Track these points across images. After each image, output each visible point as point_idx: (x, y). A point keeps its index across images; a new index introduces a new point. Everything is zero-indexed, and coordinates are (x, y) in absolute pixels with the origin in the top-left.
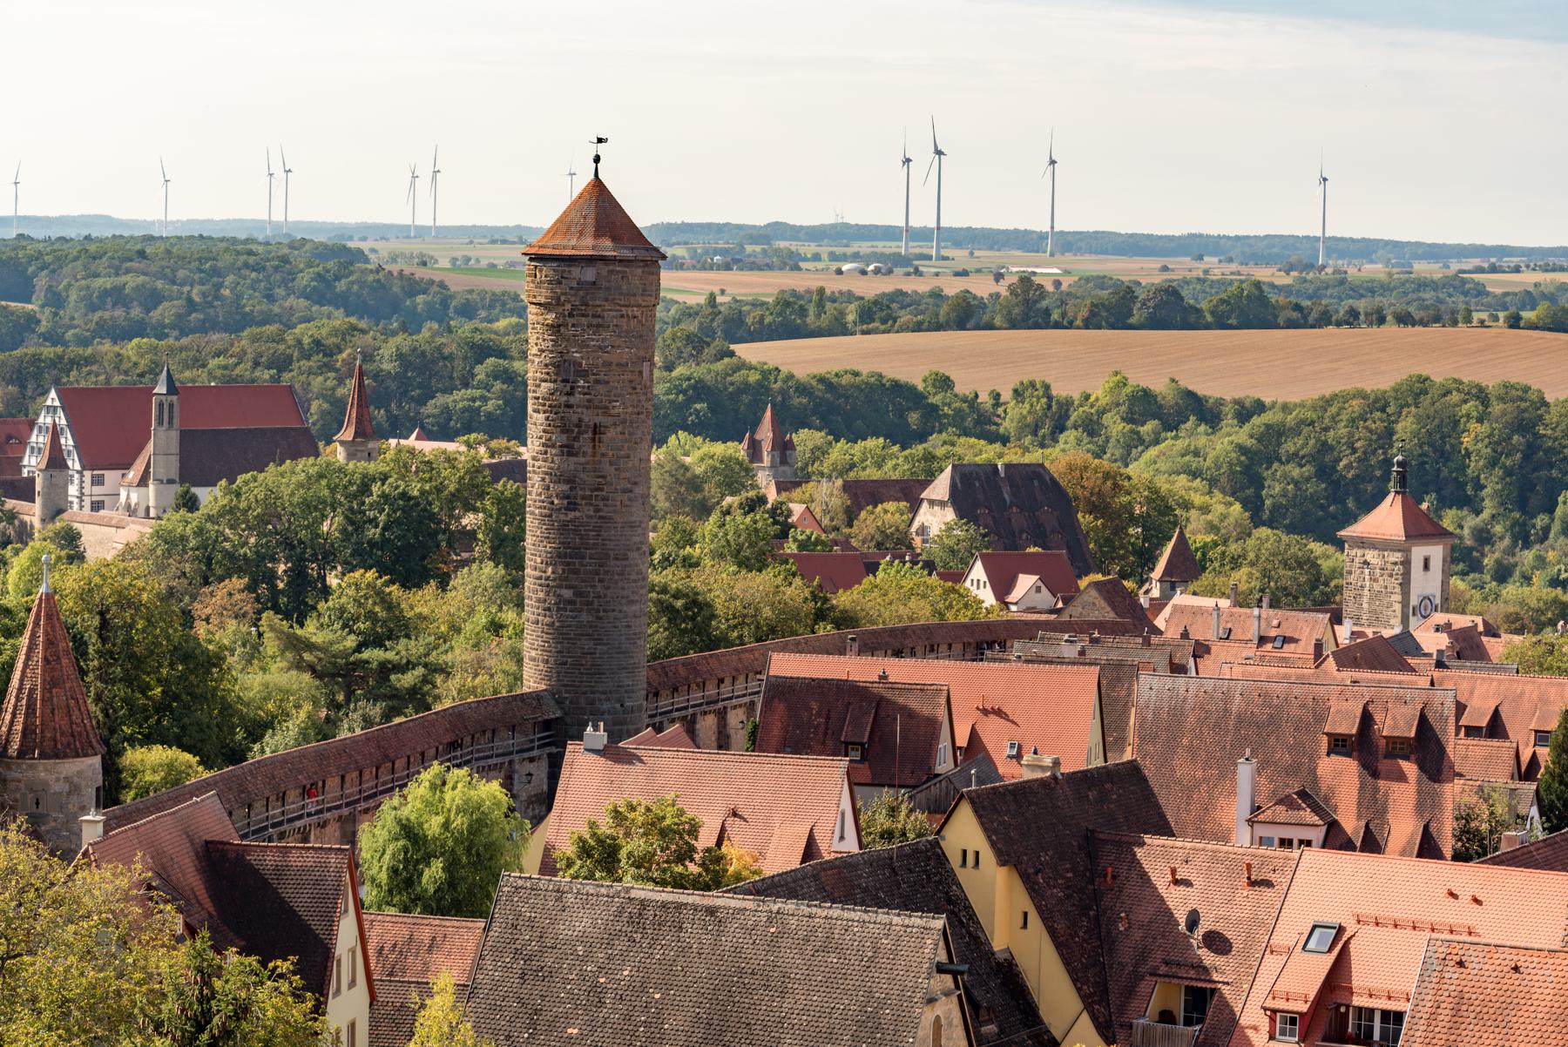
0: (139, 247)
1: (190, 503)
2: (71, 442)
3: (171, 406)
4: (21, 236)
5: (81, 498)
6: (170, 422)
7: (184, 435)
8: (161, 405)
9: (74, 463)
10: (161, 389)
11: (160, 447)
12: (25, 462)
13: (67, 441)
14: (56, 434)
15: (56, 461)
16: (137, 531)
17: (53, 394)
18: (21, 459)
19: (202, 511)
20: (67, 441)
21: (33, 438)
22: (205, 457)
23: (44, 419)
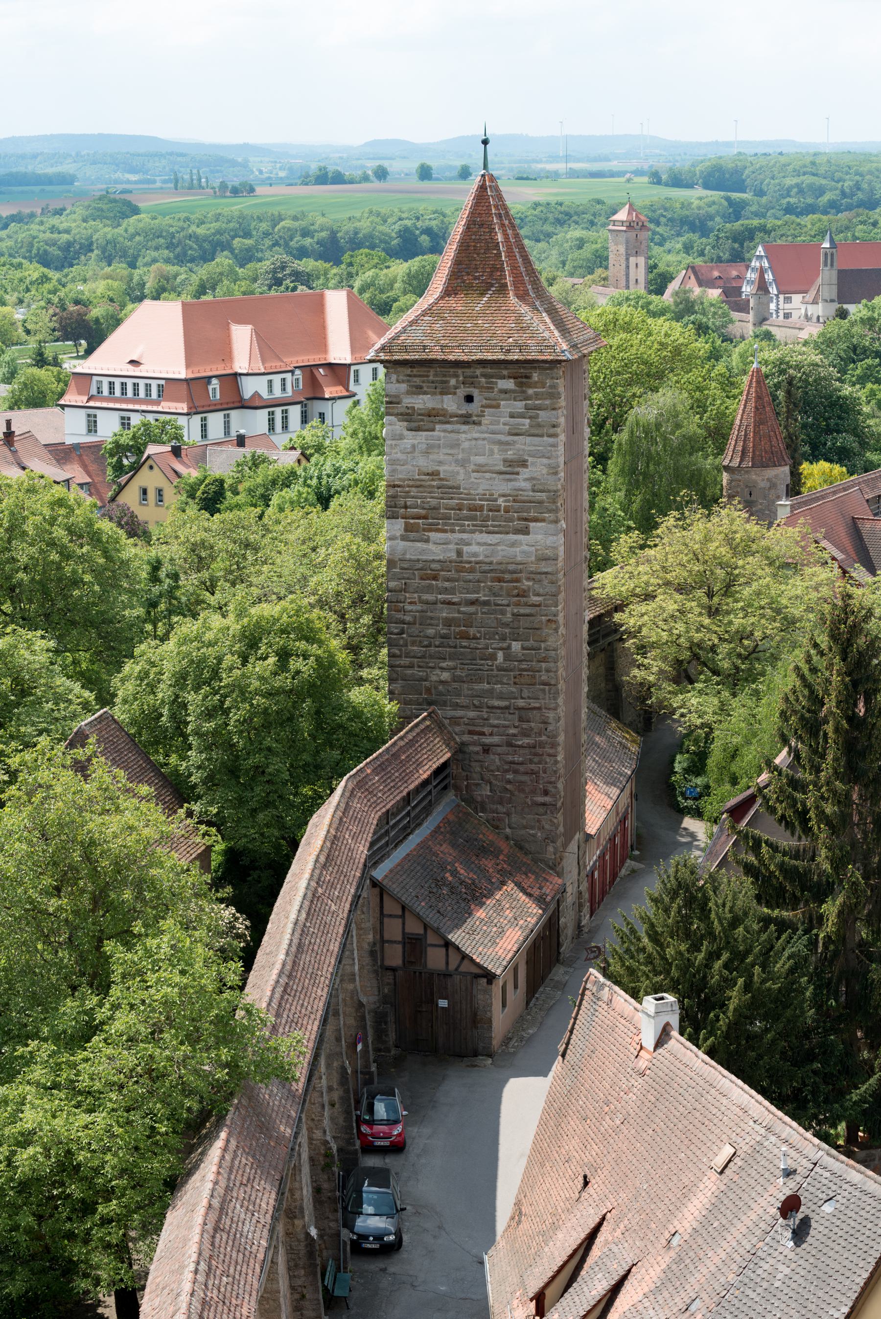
0: (811, 159)
1: (843, 314)
2: (771, 277)
3: (832, 255)
4: (740, 153)
5: (777, 311)
6: (832, 265)
7: (842, 274)
8: (826, 254)
9: (773, 290)
10: (826, 245)
11: (826, 278)
12: (744, 289)
13: (769, 277)
14: (762, 272)
15: (763, 287)
16: (812, 331)
17: (760, 248)
18: (741, 287)
19: (851, 317)
20: (769, 277)
21: (748, 275)
22: (853, 285)
23: (755, 263)
